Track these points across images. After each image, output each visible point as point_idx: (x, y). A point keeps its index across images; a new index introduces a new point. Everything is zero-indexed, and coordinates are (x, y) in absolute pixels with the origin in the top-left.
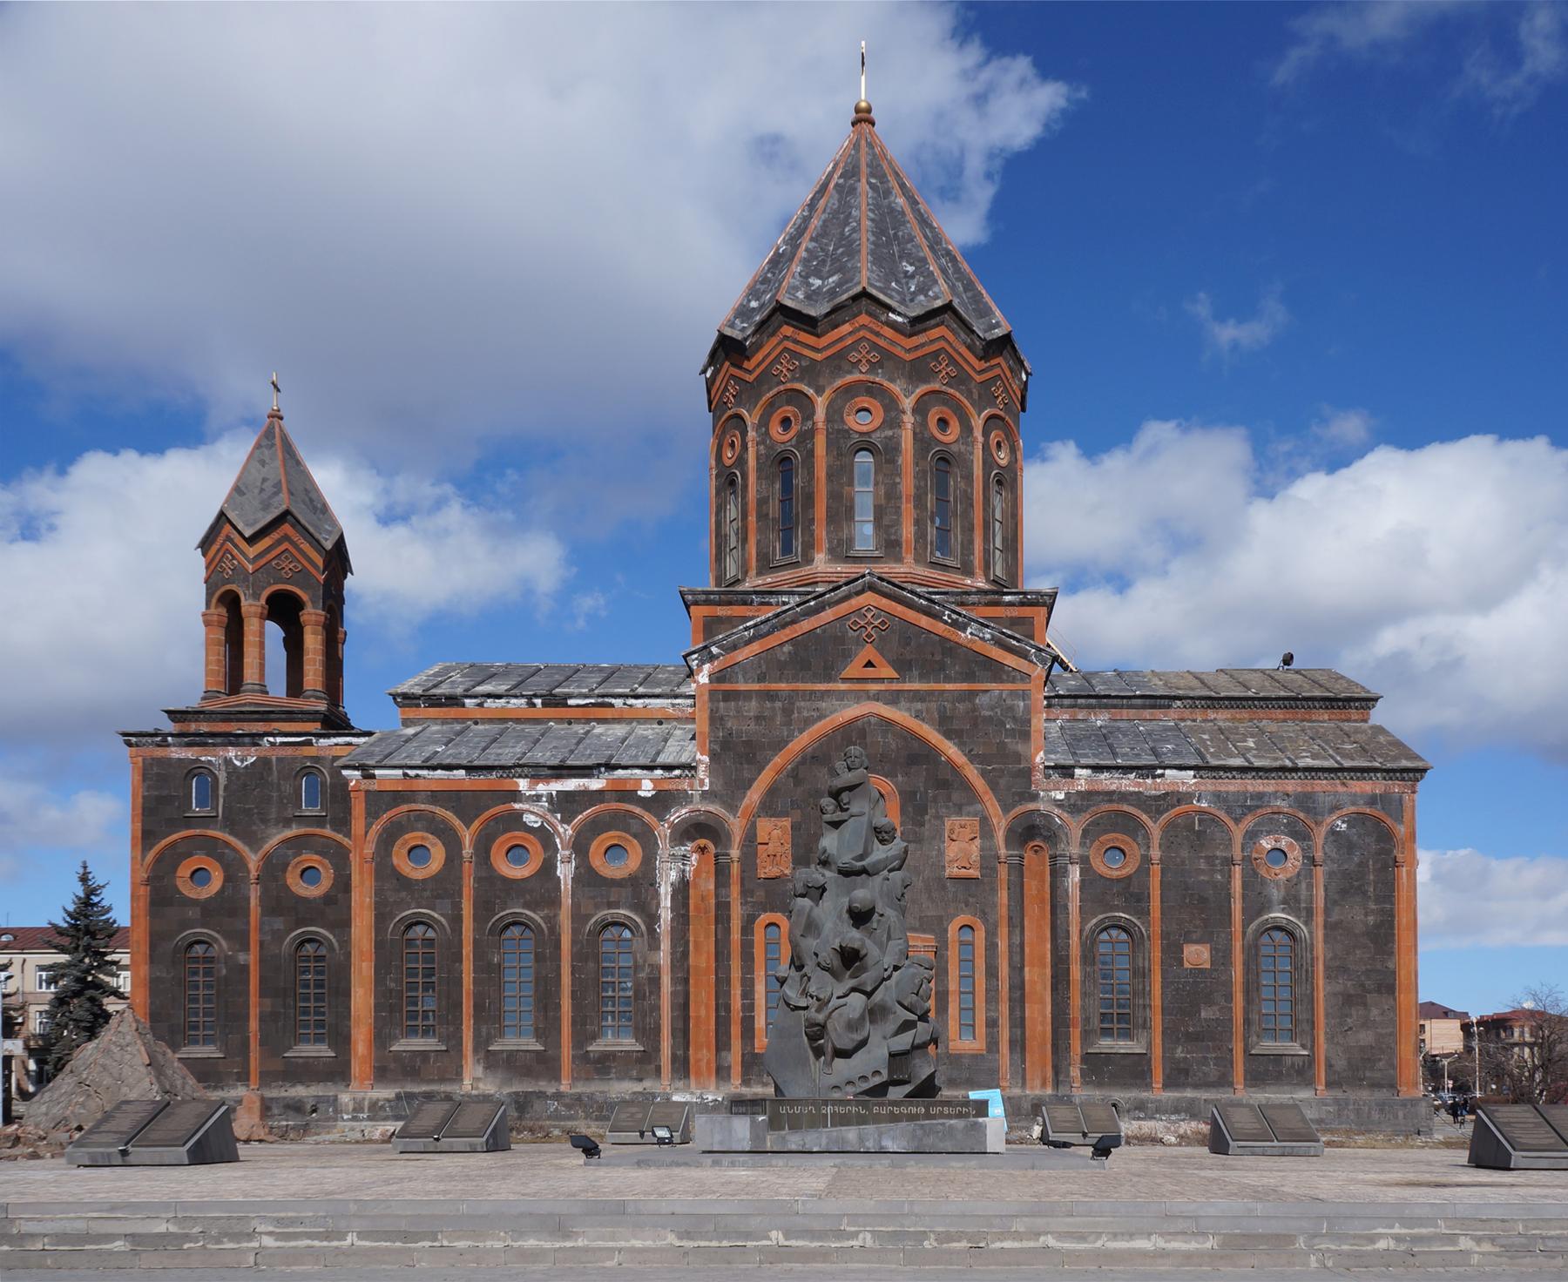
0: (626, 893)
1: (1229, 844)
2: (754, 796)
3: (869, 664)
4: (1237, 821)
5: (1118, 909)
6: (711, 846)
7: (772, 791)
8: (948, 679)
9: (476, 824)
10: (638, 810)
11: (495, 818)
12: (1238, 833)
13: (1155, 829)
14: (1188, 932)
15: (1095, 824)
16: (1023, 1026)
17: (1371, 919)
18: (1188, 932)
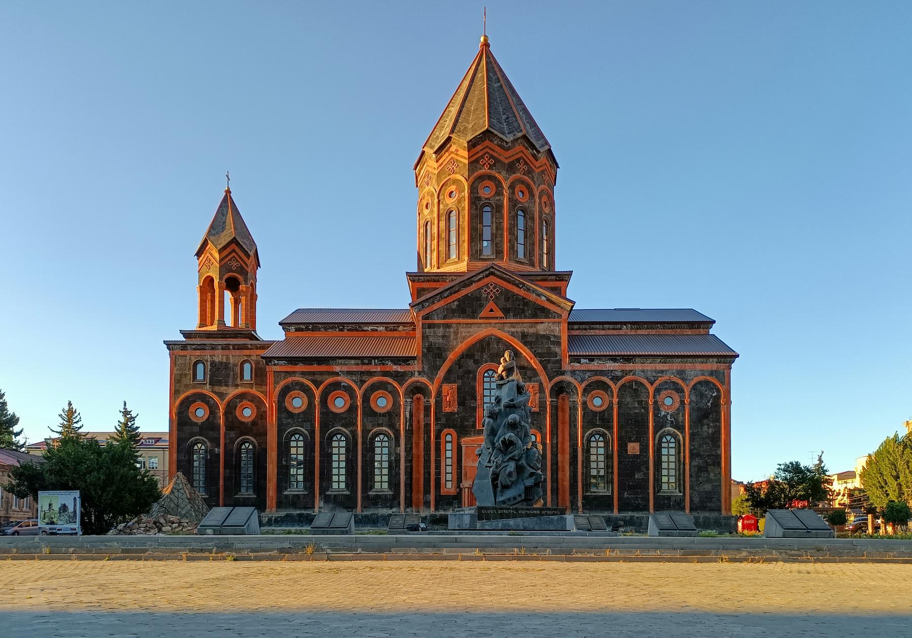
0: (386, 419)
1: (648, 397)
2: (441, 373)
3: (491, 310)
4: (652, 384)
5: (598, 426)
6: (422, 397)
7: (449, 371)
8: (525, 317)
9: (322, 387)
10: (390, 380)
11: (331, 385)
12: (651, 390)
13: (615, 388)
14: (630, 437)
15: (589, 385)
16: (557, 483)
17: (710, 431)
18: (630, 437)
